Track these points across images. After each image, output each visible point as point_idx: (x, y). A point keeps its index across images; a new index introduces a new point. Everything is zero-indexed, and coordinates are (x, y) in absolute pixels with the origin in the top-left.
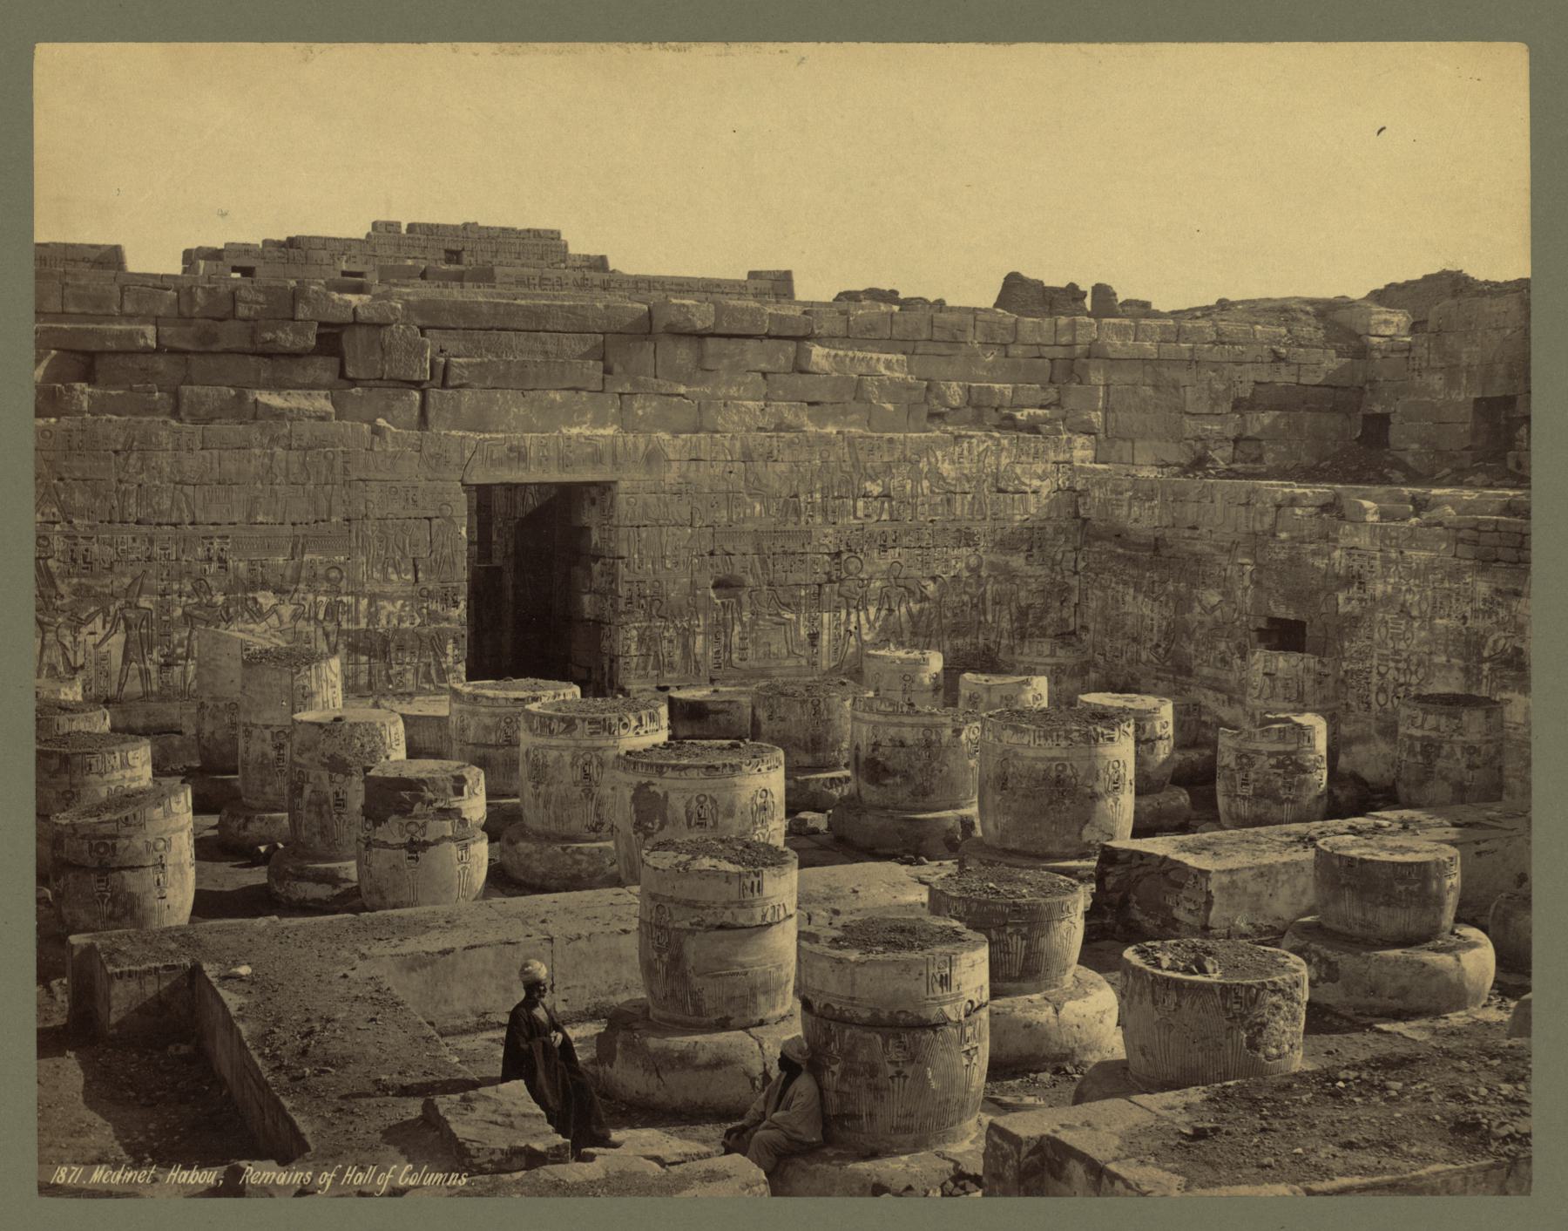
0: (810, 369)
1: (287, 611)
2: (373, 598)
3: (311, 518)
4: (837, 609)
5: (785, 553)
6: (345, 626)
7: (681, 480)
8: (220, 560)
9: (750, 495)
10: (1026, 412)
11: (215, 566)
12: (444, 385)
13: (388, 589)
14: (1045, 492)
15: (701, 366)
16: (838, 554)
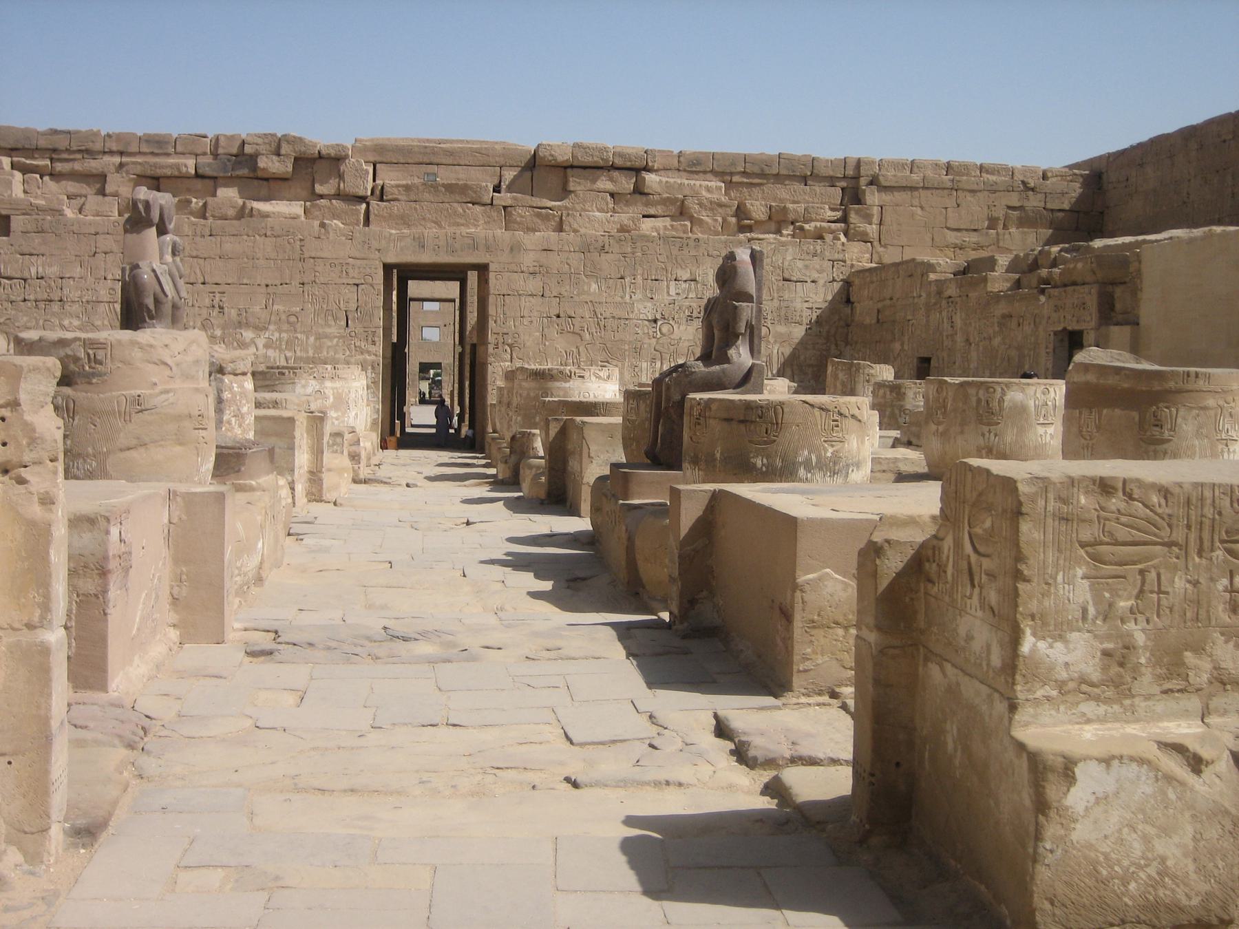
0: (646, 191)
1: (261, 342)
2: (319, 337)
3: (278, 282)
4: (653, 360)
5: (613, 317)
6: (298, 354)
7: (535, 264)
8: (220, 307)
9: (586, 276)
10: (813, 224)
11: (217, 309)
12: (381, 200)
13: (328, 330)
14: (821, 282)
15: (565, 192)
16: (655, 321)
